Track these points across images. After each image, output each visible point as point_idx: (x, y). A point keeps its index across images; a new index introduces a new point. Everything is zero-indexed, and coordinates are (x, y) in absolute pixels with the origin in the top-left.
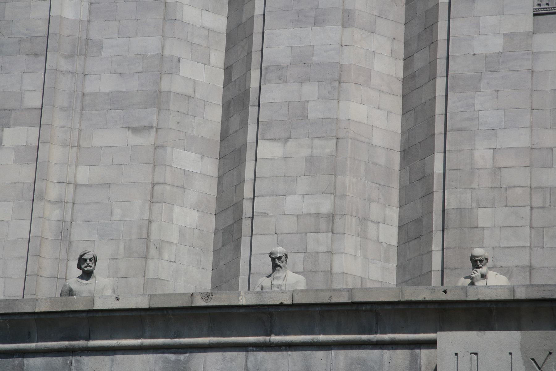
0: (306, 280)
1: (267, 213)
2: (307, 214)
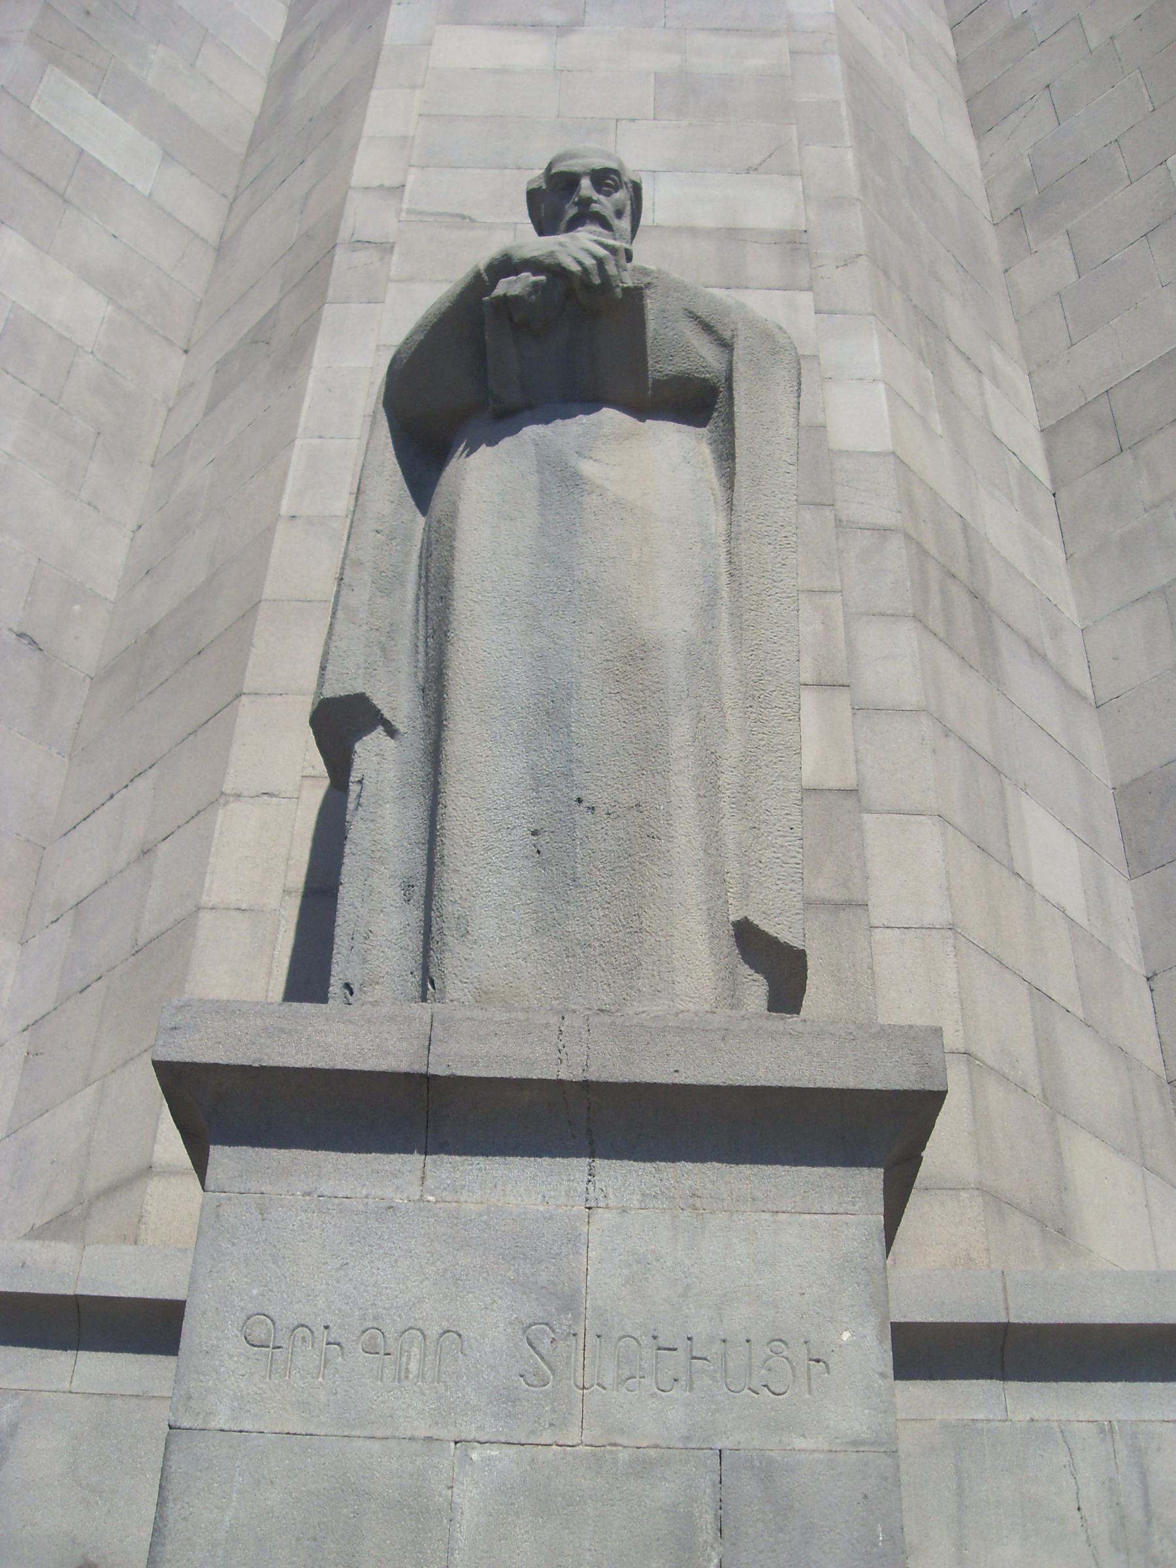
1: (466, 213)
2: (677, 230)
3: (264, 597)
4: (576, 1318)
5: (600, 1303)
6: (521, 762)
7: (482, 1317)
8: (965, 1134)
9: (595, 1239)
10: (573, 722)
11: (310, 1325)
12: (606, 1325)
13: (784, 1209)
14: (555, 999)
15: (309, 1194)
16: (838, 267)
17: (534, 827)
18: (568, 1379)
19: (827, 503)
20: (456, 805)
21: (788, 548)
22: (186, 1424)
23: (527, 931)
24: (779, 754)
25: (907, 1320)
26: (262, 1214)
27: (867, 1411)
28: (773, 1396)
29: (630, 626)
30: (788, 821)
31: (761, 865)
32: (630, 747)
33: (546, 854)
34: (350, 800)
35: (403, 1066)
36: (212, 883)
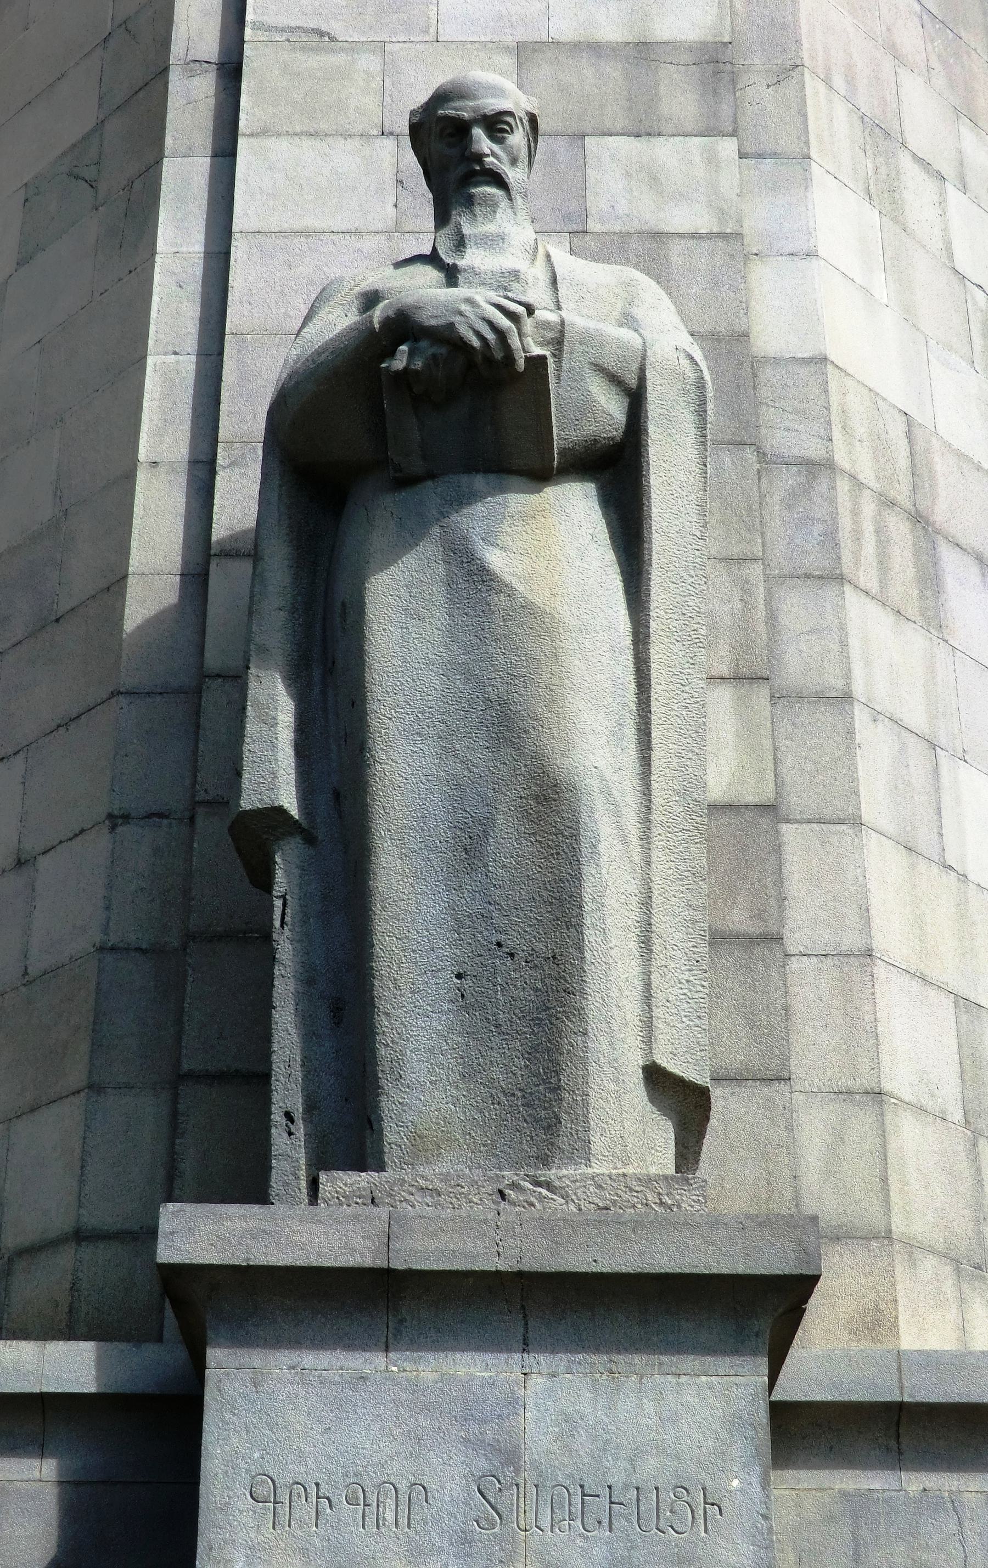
1: (324, 28)
2: (576, 47)
4: (517, 1471)
5: (536, 1457)
6: (442, 901)
7: (441, 1471)
8: (878, 1180)
9: (530, 1403)
10: (490, 861)
11: (302, 1482)
12: (541, 1476)
13: (685, 1372)
14: (484, 1146)
15: (293, 1368)
16: (768, 86)
17: (456, 969)
18: (512, 1522)
20: (383, 945)
23: (455, 1077)
25: (807, 1399)
26: (256, 1387)
27: (751, 1547)
28: (676, 1535)
29: (543, 762)
31: (668, 1004)
32: (544, 893)
33: (470, 1000)
34: (274, 917)
35: (368, 1262)
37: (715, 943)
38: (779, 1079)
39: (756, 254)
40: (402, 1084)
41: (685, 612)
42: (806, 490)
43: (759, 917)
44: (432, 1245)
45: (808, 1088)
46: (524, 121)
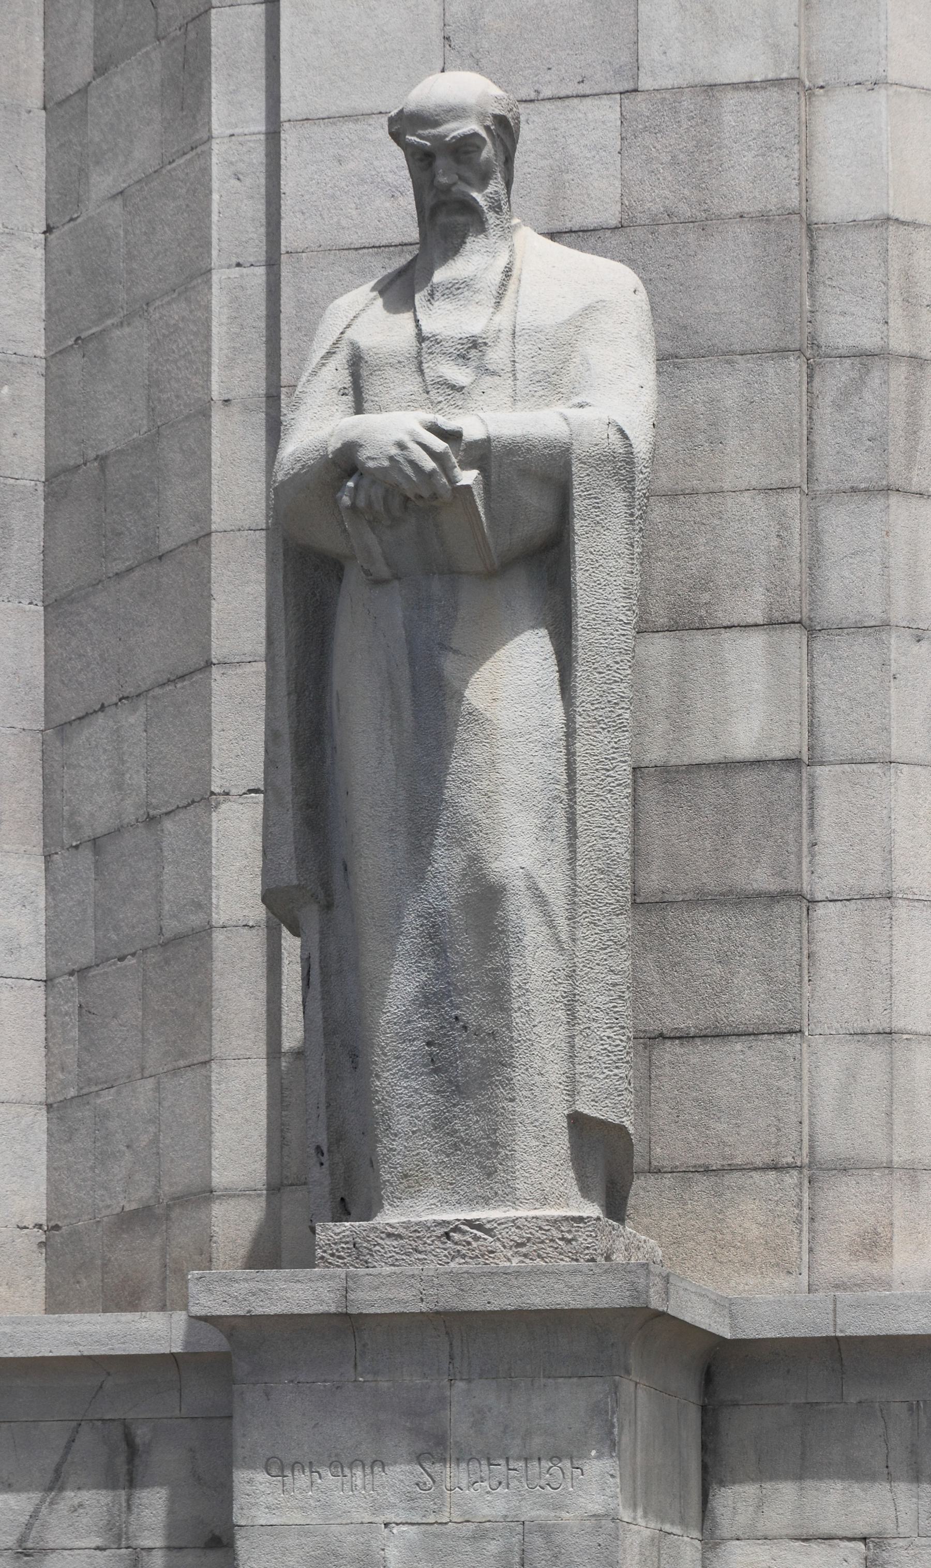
0: (646, 282)
3: (213, 527)
4: (445, 1449)
5: (458, 1439)
14: (451, 1184)
15: (292, 1381)
19: (793, 347)
21: (620, 728)
22: (242, 1524)
23: (429, 1128)
24: (609, 950)
30: (615, 1013)
35: (333, 1310)
36: (218, 897)
37: (740, 903)
38: (791, 1032)
39: (822, 87)
40: (392, 1134)
41: (610, 699)
42: (858, 385)
43: (779, 874)
44: (376, 1295)
45: (827, 1032)
46: (492, 128)
